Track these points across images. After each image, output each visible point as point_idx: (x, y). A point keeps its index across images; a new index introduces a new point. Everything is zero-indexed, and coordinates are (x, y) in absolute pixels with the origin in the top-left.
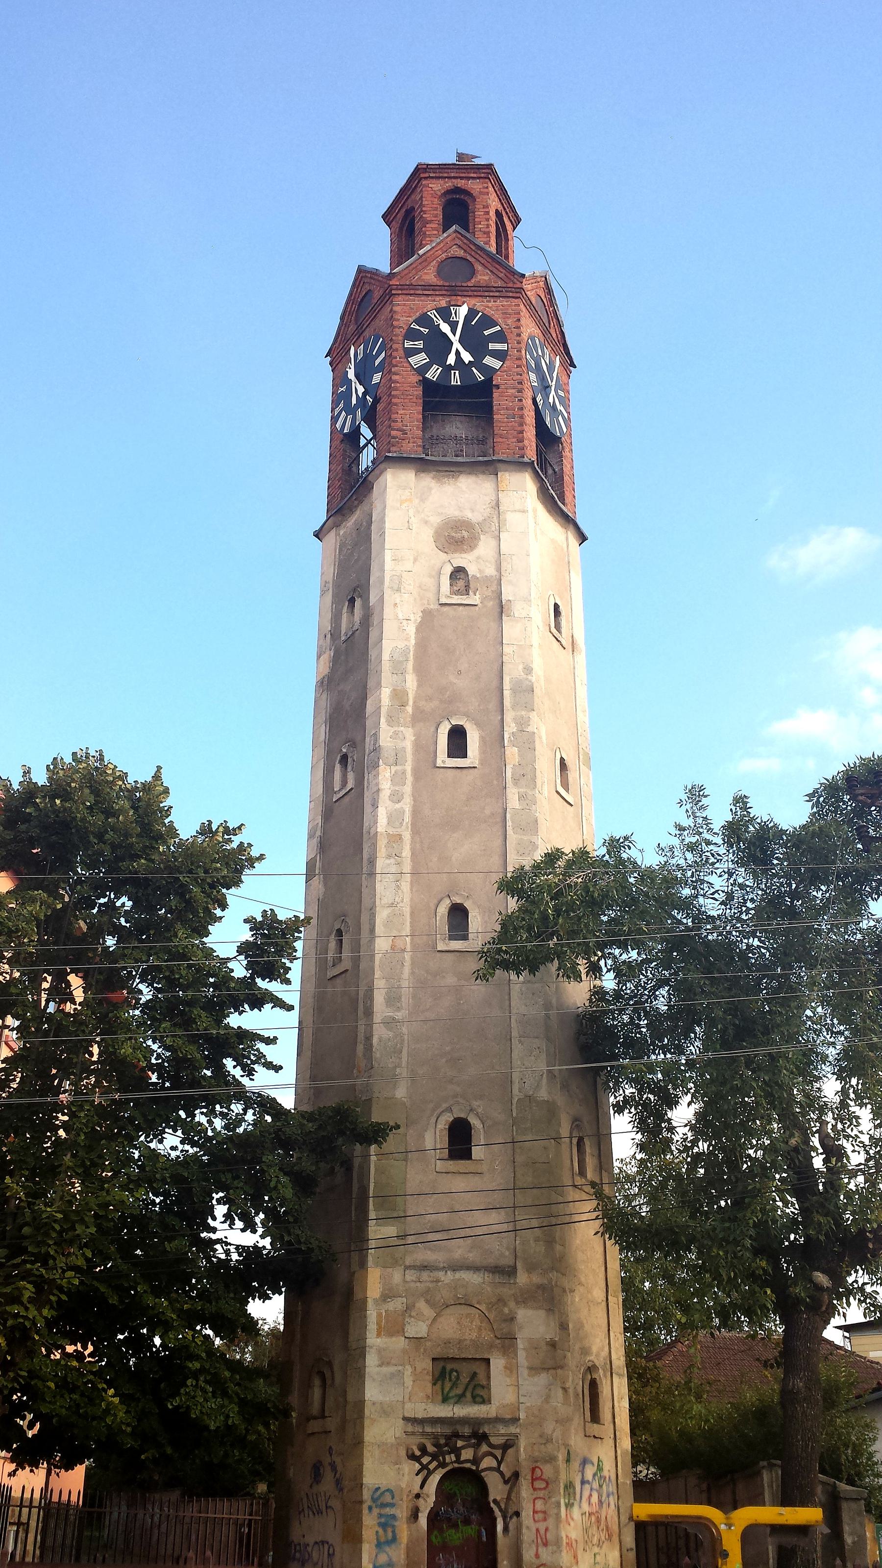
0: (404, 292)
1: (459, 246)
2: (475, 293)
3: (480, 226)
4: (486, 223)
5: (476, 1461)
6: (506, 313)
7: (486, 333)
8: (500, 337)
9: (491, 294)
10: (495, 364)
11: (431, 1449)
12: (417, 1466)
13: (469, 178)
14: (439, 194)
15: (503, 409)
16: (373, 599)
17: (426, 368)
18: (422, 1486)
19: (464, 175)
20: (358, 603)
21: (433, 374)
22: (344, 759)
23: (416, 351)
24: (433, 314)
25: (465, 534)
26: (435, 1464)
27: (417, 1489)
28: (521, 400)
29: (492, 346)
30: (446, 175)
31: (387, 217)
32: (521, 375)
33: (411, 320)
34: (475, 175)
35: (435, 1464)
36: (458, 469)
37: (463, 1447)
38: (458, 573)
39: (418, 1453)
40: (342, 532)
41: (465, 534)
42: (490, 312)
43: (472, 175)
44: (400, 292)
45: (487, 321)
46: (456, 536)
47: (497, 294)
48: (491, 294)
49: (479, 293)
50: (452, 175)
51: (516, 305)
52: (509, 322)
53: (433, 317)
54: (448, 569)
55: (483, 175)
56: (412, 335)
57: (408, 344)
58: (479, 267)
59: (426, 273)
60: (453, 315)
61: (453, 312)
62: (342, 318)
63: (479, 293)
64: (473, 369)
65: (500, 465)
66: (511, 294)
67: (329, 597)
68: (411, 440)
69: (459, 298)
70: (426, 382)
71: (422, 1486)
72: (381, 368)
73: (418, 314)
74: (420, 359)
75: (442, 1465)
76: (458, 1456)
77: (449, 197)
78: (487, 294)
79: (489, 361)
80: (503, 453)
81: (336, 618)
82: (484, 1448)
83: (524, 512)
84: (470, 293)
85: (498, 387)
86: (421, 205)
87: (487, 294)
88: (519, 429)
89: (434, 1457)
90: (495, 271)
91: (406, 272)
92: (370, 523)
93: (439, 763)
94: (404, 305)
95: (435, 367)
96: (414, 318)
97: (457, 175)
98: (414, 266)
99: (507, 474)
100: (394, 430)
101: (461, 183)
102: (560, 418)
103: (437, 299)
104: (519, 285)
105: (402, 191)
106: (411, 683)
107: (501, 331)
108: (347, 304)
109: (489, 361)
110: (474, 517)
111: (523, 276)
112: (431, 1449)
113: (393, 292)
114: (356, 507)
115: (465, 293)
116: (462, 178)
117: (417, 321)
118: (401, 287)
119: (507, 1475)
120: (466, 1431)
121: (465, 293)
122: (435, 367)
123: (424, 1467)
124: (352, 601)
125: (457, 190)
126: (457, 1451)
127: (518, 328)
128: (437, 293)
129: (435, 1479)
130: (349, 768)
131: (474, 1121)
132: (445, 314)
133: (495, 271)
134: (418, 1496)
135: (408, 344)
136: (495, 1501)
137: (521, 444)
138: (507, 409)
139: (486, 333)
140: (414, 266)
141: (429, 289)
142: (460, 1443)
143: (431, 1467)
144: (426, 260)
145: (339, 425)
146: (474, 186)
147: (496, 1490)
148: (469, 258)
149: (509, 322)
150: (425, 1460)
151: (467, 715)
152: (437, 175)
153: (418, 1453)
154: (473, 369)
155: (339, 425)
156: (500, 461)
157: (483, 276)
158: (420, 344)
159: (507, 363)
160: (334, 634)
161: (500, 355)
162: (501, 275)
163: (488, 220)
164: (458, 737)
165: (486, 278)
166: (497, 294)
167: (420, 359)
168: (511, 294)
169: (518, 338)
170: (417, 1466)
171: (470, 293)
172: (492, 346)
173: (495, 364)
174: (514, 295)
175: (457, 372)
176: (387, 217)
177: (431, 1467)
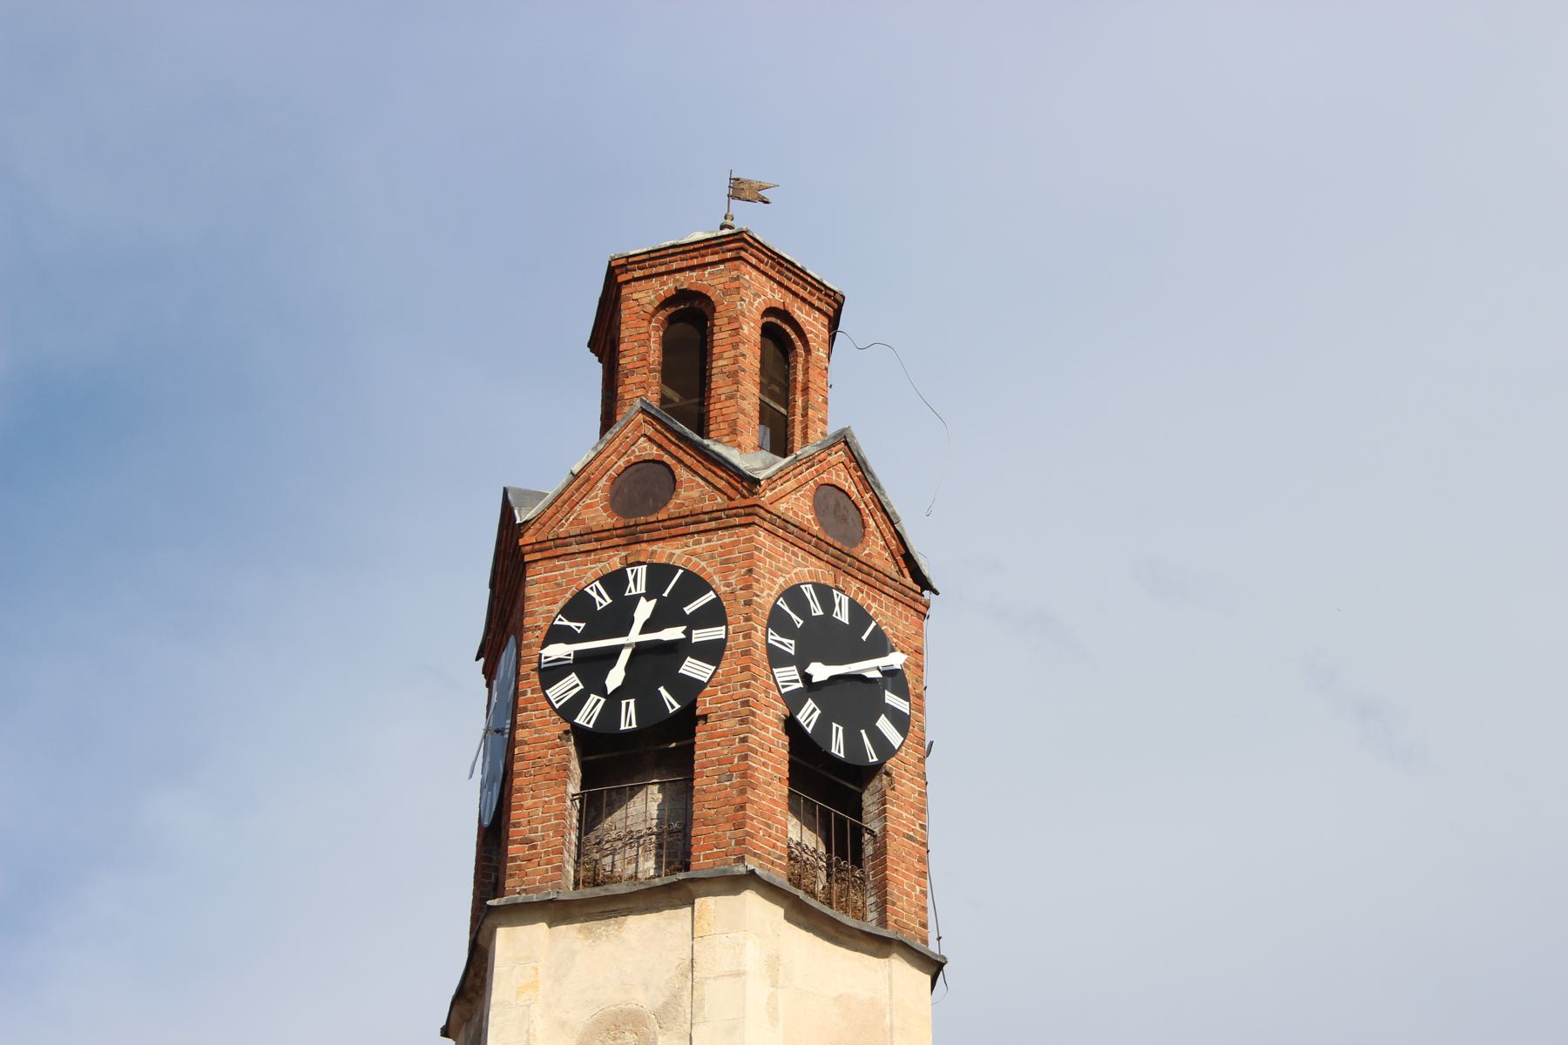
0: (547, 554)
1: (650, 439)
2: (673, 531)
3: (721, 363)
4: (732, 353)
6: (727, 561)
7: (688, 610)
8: (714, 614)
9: (702, 527)
13: (704, 266)
14: (650, 309)
15: (712, 763)
17: (577, 703)
19: (695, 262)
28: (744, 740)
30: (663, 269)
32: (748, 686)
33: (557, 608)
34: (716, 258)
36: (623, 906)
43: (709, 259)
44: (538, 556)
45: (694, 584)
47: (713, 524)
48: (702, 527)
49: (680, 530)
50: (674, 266)
51: (747, 541)
53: (594, 594)
55: (729, 255)
58: (682, 474)
59: (589, 506)
60: (631, 584)
61: (631, 578)
62: (492, 585)
63: (680, 530)
64: (662, 689)
65: (691, 887)
66: (737, 521)
68: (544, 858)
69: (644, 546)
70: (578, 731)
73: (569, 595)
77: (671, 310)
78: (692, 528)
80: (706, 857)
83: (739, 974)
84: (664, 533)
85: (705, 717)
87: (692, 528)
88: (738, 800)
90: (711, 477)
91: (550, 512)
94: (546, 580)
95: (593, 698)
96: (561, 604)
97: (684, 264)
98: (565, 496)
99: (710, 900)
100: (515, 842)
101: (689, 280)
102: (884, 724)
104: (749, 502)
110: (644, 1000)
111: (757, 482)
113: (527, 558)
115: (655, 535)
116: (692, 268)
117: (567, 612)
118: (540, 546)
121: (655, 535)
122: (593, 698)
125: (682, 295)
127: (748, 587)
128: (605, 544)
133: (711, 477)
137: (739, 833)
138: (720, 762)
139: (688, 610)
140: (565, 496)
141: (594, 538)
144: (588, 479)
146: (709, 281)
148: (666, 458)
152: (647, 272)
154: (662, 689)
159: (725, 666)
161: (712, 653)
162: (722, 484)
163: (735, 346)
165: (695, 494)
166: (713, 524)
168: (737, 521)
169: (747, 609)
171: (664, 533)
174: (744, 520)
175: (632, 701)
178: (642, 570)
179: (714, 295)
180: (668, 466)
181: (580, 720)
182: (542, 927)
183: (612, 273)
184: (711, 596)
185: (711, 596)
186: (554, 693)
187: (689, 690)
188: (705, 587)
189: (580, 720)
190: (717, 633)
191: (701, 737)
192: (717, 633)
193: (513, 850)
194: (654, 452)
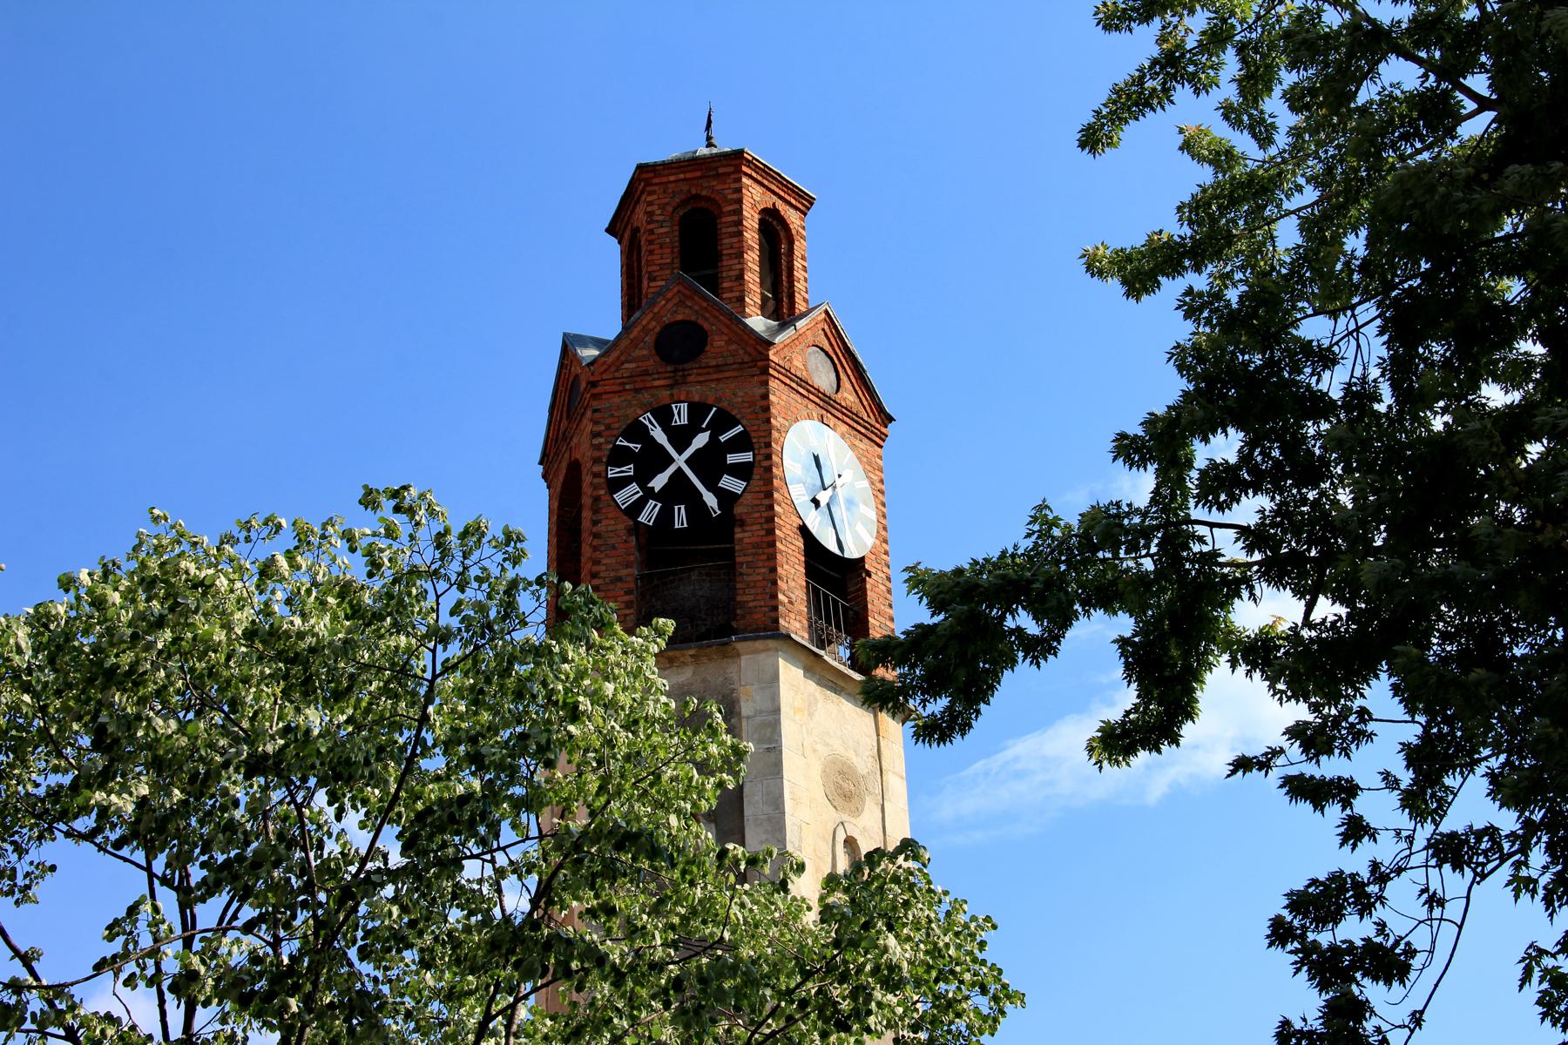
7: (723, 438)
17: (638, 506)
24: (647, 419)
29: (732, 459)
56: (620, 457)
57: (613, 473)
74: (627, 495)
79: (729, 483)
109: (729, 483)
122: (652, 503)
132: (664, 416)
135: (613, 473)
139: (723, 438)
158: (629, 471)
161: (741, 471)
167: (627, 495)
172: (732, 459)
176: (611, 230)
178: (684, 407)
181: (642, 519)
184: (740, 428)
185: (740, 428)
186: (619, 497)
187: (726, 498)
189: (642, 519)
190: (747, 457)
192: (747, 457)
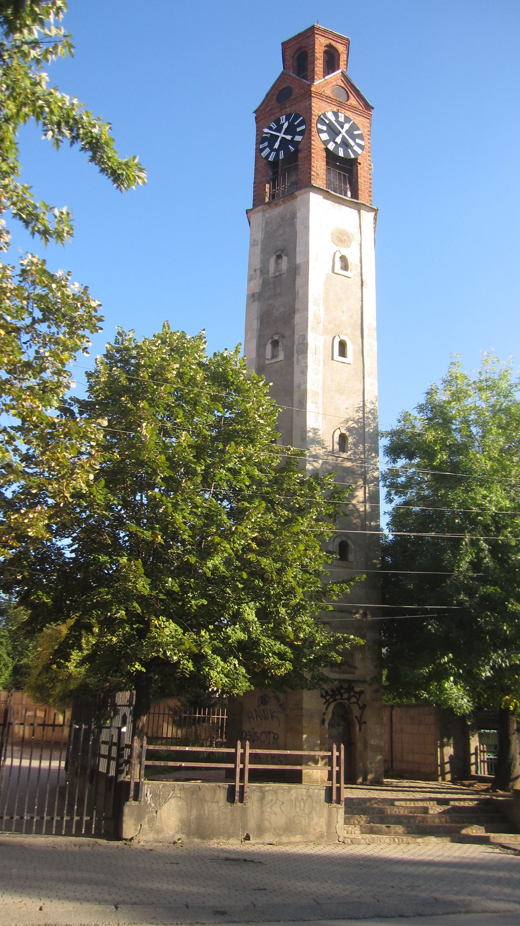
5: (349, 699)
10: (359, 151)
11: (330, 693)
12: (324, 700)
16: (299, 260)
18: (326, 709)
20: (285, 259)
21: (331, 146)
22: (275, 344)
23: (323, 131)
25: (346, 238)
26: (332, 699)
27: (324, 710)
31: (285, 45)
35: (332, 699)
37: (344, 693)
38: (343, 259)
39: (324, 694)
40: (267, 215)
41: (346, 238)
42: (356, 122)
46: (341, 238)
52: (365, 130)
54: (338, 256)
62: (267, 95)
65: (362, 206)
67: (258, 249)
70: (327, 150)
71: (326, 709)
72: (301, 133)
75: (335, 700)
76: (342, 696)
81: (265, 262)
82: (352, 693)
86: (314, 48)
89: (331, 696)
92: (294, 216)
93: (335, 359)
101: (333, 43)
103: (333, 106)
105: (299, 35)
106: (322, 313)
107: (361, 134)
108: (272, 88)
112: (330, 693)
114: (280, 205)
116: (334, 41)
119: (361, 705)
120: (346, 686)
123: (327, 701)
124: (279, 257)
126: (341, 694)
129: (332, 706)
130: (280, 348)
131: (350, 543)
134: (324, 714)
135: (319, 126)
136: (356, 717)
142: (343, 691)
143: (330, 701)
145: (264, 154)
146: (341, 48)
147: (356, 711)
149: (365, 130)
150: (328, 698)
151: (346, 335)
153: (324, 694)
155: (264, 154)
156: (363, 204)
157: (353, 101)
160: (264, 271)
164: (343, 345)
170: (324, 700)
173: (359, 151)
177: (330, 701)
178: (343, 115)
179: (340, 52)
180: (347, 92)
182: (321, 197)
183: (313, 27)
186: (321, 135)
188: (358, 129)
191: (359, 167)
193: (312, 173)
194: (343, 85)
